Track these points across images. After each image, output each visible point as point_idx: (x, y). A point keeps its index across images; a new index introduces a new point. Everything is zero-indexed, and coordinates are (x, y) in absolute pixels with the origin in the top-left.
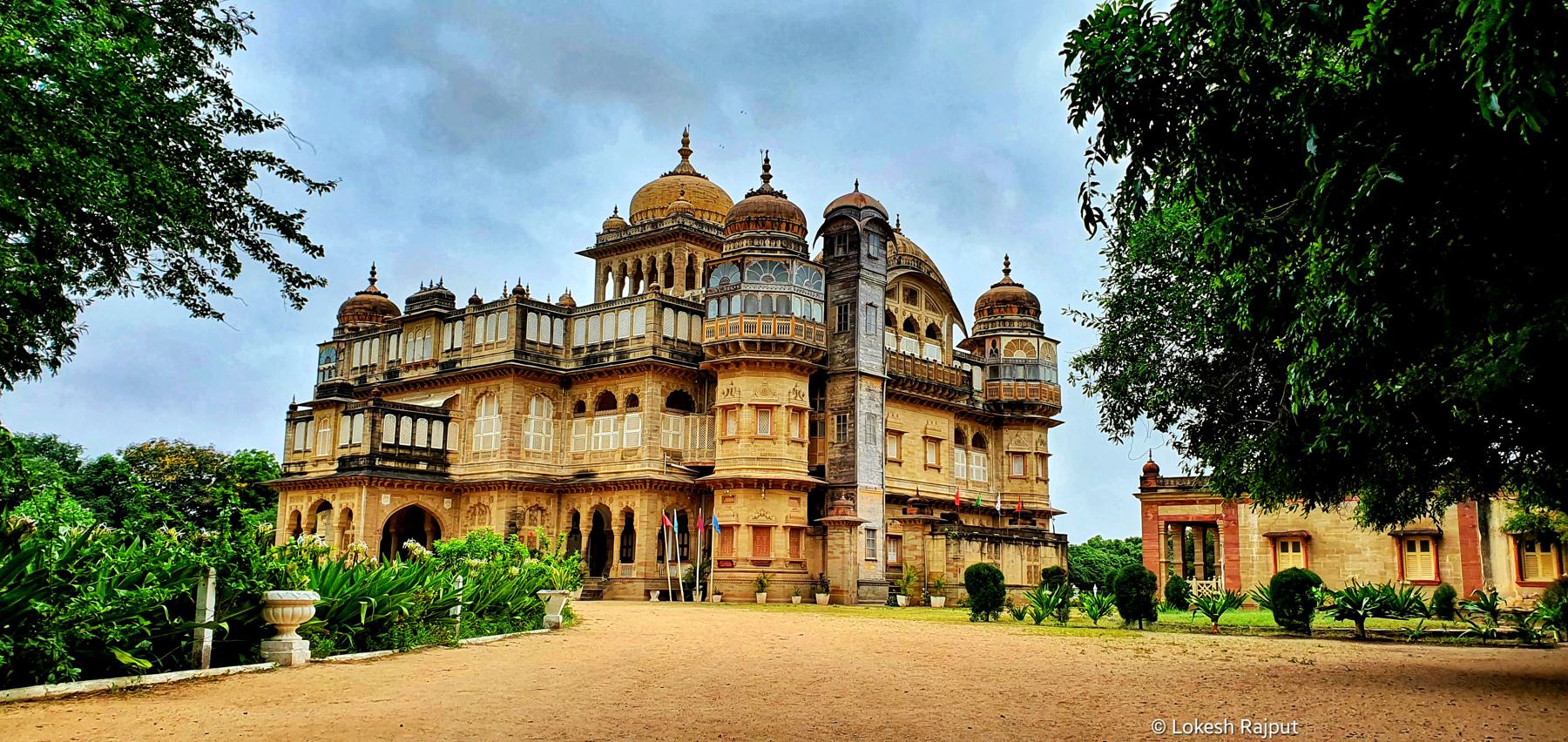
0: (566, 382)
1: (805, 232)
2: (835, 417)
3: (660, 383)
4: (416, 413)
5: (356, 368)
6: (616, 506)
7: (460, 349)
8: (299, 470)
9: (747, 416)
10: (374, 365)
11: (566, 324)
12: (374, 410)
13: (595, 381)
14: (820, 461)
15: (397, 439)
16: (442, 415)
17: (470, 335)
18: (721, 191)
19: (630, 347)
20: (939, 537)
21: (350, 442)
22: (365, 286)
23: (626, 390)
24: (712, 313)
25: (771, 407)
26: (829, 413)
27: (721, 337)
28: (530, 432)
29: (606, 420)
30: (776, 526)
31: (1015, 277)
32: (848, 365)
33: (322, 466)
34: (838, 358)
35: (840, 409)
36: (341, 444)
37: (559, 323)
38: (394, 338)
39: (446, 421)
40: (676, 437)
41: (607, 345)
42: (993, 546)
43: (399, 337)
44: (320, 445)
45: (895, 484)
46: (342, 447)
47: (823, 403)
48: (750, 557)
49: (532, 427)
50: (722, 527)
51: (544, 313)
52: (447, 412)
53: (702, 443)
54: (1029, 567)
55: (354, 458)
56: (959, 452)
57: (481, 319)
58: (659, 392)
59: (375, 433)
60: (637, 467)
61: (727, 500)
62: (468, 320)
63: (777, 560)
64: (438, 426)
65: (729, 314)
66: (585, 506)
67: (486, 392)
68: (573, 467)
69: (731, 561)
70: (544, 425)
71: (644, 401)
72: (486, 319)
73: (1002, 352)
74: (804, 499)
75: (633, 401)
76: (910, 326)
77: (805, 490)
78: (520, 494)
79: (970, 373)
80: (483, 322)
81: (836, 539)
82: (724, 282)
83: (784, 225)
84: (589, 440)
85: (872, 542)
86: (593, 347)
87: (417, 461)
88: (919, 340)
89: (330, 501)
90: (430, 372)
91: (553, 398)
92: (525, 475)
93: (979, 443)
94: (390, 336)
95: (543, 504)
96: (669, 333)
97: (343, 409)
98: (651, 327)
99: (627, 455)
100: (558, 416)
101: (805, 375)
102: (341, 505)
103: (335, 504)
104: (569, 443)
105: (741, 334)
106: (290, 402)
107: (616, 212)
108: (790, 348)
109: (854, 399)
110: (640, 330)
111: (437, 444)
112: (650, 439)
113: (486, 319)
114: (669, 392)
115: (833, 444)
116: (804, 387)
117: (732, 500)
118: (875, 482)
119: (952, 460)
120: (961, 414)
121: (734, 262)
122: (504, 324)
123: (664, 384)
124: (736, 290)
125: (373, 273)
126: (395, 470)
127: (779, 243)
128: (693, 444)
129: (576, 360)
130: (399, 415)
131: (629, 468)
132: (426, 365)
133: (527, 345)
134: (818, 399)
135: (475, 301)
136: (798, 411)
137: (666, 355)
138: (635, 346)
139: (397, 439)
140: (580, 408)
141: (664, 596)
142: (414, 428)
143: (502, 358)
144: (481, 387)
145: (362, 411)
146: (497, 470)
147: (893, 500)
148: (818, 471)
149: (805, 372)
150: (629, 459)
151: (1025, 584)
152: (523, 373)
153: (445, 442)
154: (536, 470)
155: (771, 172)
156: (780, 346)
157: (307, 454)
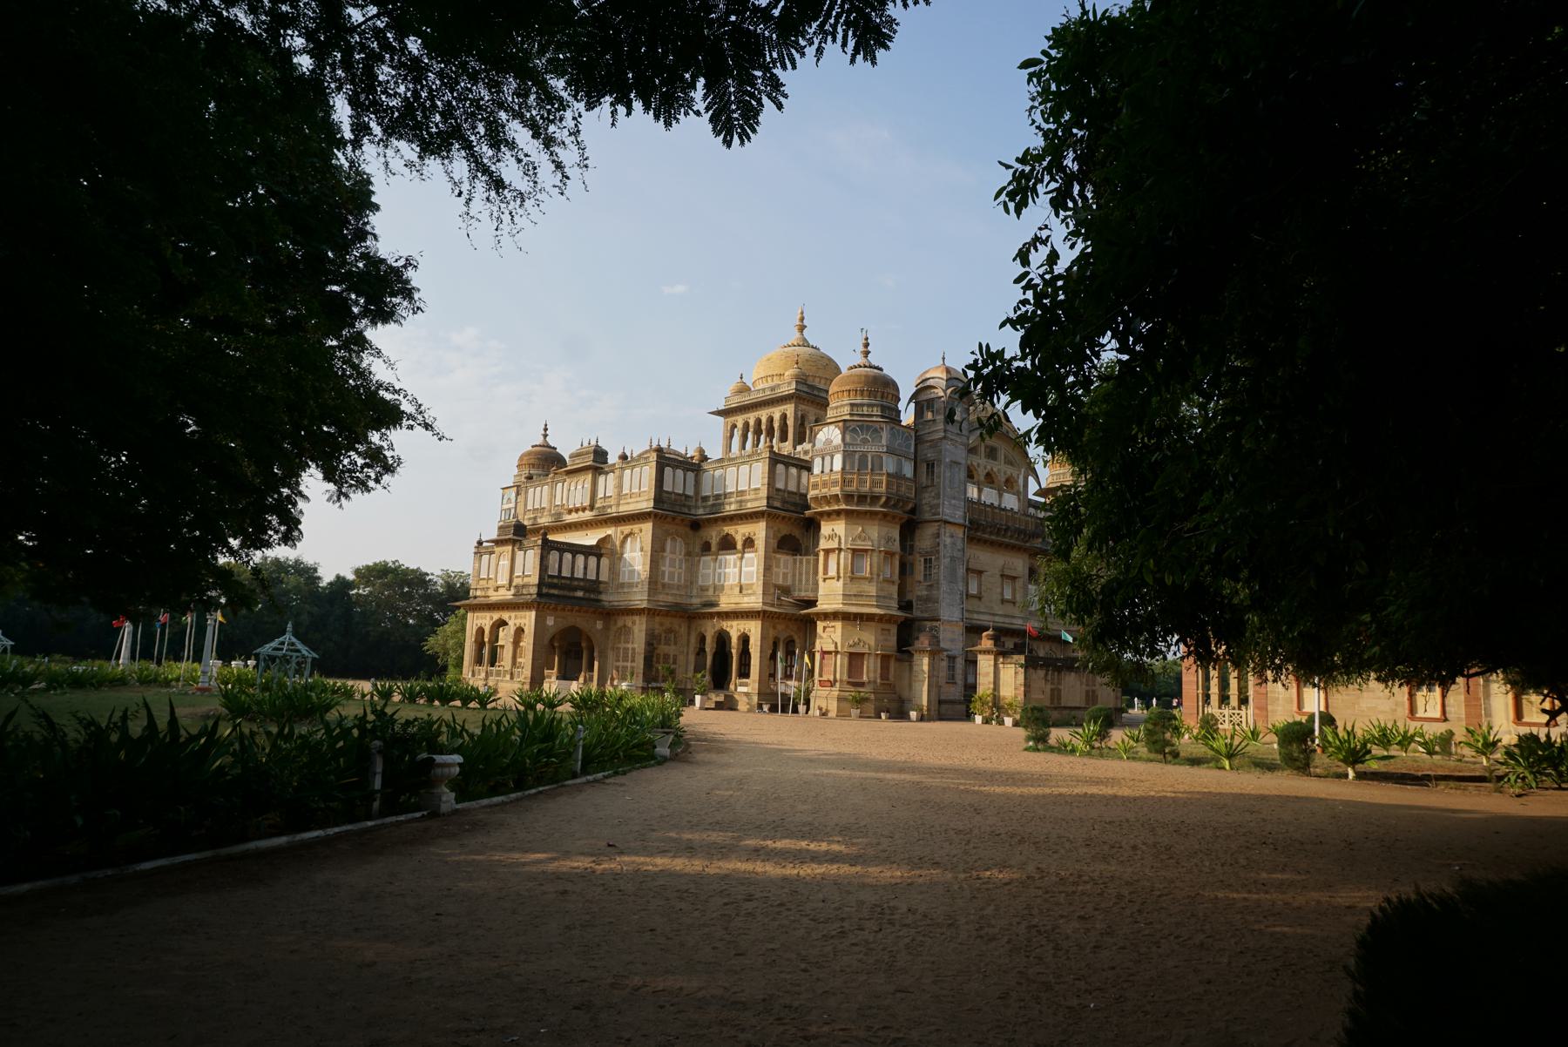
1: (899, 400)
6: (734, 629)
11: (696, 476)
14: (909, 597)
17: (620, 486)
18: (830, 360)
19: (748, 497)
22: (540, 441)
26: (918, 555)
28: (666, 568)
32: (934, 514)
33: (502, 591)
37: (691, 475)
38: (560, 485)
40: (785, 575)
44: (499, 575)
45: (976, 616)
47: (912, 547)
51: (677, 467)
52: (600, 549)
53: (807, 580)
54: (1087, 692)
60: (753, 599)
62: (617, 472)
64: (593, 561)
65: (831, 470)
74: (894, 630)
75: (749, 543)
76: (990, 479)
77: (895, 622)
78: (657, 619)
83: (879, 394)
85: (952, 668)
87: (575, 589)
90: (588, 515)
98: (766, 481)
100: (688, 554)
101: (896, 523)
103: (511, 623)
106: (478, 539)
108: (883, 499)
109: (939, 544)
111: (592, 576)
114: (780, 535)
116: (896, 534)
118: (957, 615)
120: (1033, 553)
123: (776, 529)
125: (546, 430)
128: (800, 580)
129: (704, 507)
131: (746, 599)
135: (624, 457)
138: (753, 497)
140: (706, 548)
144: (627, 529)
148: (906, 606)
149: (897, 520)
153: (598, 574)
154: (670, 599)
156: (875, 499)
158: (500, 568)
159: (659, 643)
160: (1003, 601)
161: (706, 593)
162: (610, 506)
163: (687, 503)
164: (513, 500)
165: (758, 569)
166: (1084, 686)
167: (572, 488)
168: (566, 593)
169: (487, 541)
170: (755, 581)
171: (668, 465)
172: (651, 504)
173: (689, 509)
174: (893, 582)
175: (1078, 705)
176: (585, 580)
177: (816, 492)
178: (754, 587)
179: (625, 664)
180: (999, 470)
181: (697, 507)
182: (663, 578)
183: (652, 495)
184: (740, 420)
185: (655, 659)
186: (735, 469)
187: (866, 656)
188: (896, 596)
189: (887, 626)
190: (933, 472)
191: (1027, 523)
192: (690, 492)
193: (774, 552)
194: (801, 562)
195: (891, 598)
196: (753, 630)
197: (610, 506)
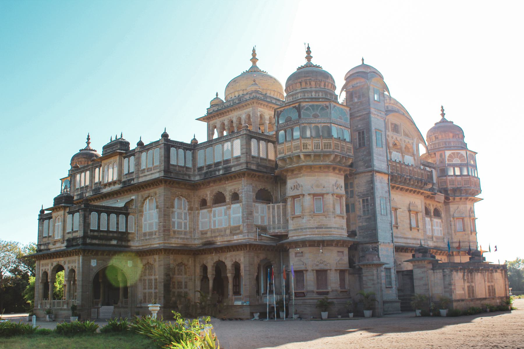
0: (195, 186)
1: (335, 88)
2: (361, 200)
3: (251, 184)
4: (109, 211)
5: (78, 189)
6: (228, 259)
7: (133, 172)
8: (46, 248)
9: (307, 201)
10: (87, 187)
11: (193, 153)
12: (84, 210)
13: (212, 186)
14: (353, 228)
15: (99, 227)
16: (124, 211)
17: (138, 164)
19: (232, 164)
20: (438, 271)
23: (231, 191)
24: (281, 139)
26: (357, 198)
27: (287, 154)
28: (175, 220)
29: (220, 210)
30: (330, 270)
31: (448, 118)
32: (367, 167)
33: (58, 245)
34: (361, 163)
35: (364, 195)
37: (189, 153)
38: (97, 170)
39: (127, 215)
40: (263, 218)
41: (218, 164)
42: (469, 274)
43: (100, 169)
46: (69, 233)
47: (352, 192)
48: (315, 290)
49: (176, 217)
50: (296, 272)
51: (179, 148)
52: (127, 210)
53: (279, 221)
54: (489, 286)
55: (74, 239)
56: (428, 219)
57: (144, 154)
58: (251, 190)
59: (86, 223)
60: (240, 236)
61: (298, 255)
62: (137, 155)
63: (332, 291)
64: (122, 218)
66: (210, 261)
67: (149, 196)
68: (201, 239)
69: (303, 293)
70: (183, 214)
71: (242, 196)
72: (147, 153)
73: (446, 160)
74: (346, 251)
75: (235, 197)
77: (347, 246)
78: (172, 257)
80: (145, 156)
81: (368, 275)
82: (288, 120)
84: (210, 222)
85: (388, 276)
86: (209, 166)
87: (111, 239)
88: (402, 153)
89: (63, 265)
90: (117, 187)
91: (187, 197)
92: (173, 245)
93: (437, 214)
94: (95, 169)
95: (185, 261)
96: (254, 153)
97: (68, 210)
98: (244, 150)
99: (235, 230)
100: (191, 209)
101: (342, 175)
102: (69, 268)
104: (198, 225)
105: (301, 150)
110: (237, 152)
111: (122, 229)
112: (248, 219)
113: (147, 153)
114: (257, 190)
115: (361, 216)
117: (301, 254)
119: (424, 224)
121: (294, 107)
122: (158, 154)
124: (297, 123)
126: (98, 245)
127: (320, 94)
128: (274, 222)
129: (200, 175)
130: (99, 213)
131: (235, 237)
132: (114, 183)
133: (171, 167)
134: (349, 190)
135: (140, 144)
136: (340, 196)
137: (254, 167)
138: (235, 163)
139: (99, 227)
140: (204, 204)
141: (263, 316)
142: (108, 220)
143: (157, 176)
144: (146, 193)
146: (156, 243)
147: (399, 249)
149: (342, 173)
150: (234, 232)
151: (488, 297)
152: (169, 183)
153: (127, 227)
154: (180, 241)
155: (311, 55)
156: (326, 155)
157: (50, 238)
158: (56, 228)
159: (174, 274)
161: (205, 236)
162: (133, 179)
163: (188, 173)
164: (68, 186)
165: (243, 215)
166: (486, 283)
167: (106, 169)
168: (104, 242)
169: (47, 210)
170: (241, 223)
171: (173, 146)
172: (162, 174)
173: (189, 177)
174: (343, 217)
175: (484, 297)
176: (117, 232)
177: (283, 155)
178: (241, 228)
179: (150, 291)
180: (400, 139)
181: (195, 176)
182: (174, 227)
183: (162, 167)
184: (218, 121)
185: (171, 286)
186: (220, 145)
187: (329, 271)
188: (345, 227)
189: (341, 249)
190: (363, 138)
191: (422, 174)
192: (189, 165)
193: (254, 202)
194: (273, 208)
195: (343, 229)
196: (242, 259)
197: (133, 179)
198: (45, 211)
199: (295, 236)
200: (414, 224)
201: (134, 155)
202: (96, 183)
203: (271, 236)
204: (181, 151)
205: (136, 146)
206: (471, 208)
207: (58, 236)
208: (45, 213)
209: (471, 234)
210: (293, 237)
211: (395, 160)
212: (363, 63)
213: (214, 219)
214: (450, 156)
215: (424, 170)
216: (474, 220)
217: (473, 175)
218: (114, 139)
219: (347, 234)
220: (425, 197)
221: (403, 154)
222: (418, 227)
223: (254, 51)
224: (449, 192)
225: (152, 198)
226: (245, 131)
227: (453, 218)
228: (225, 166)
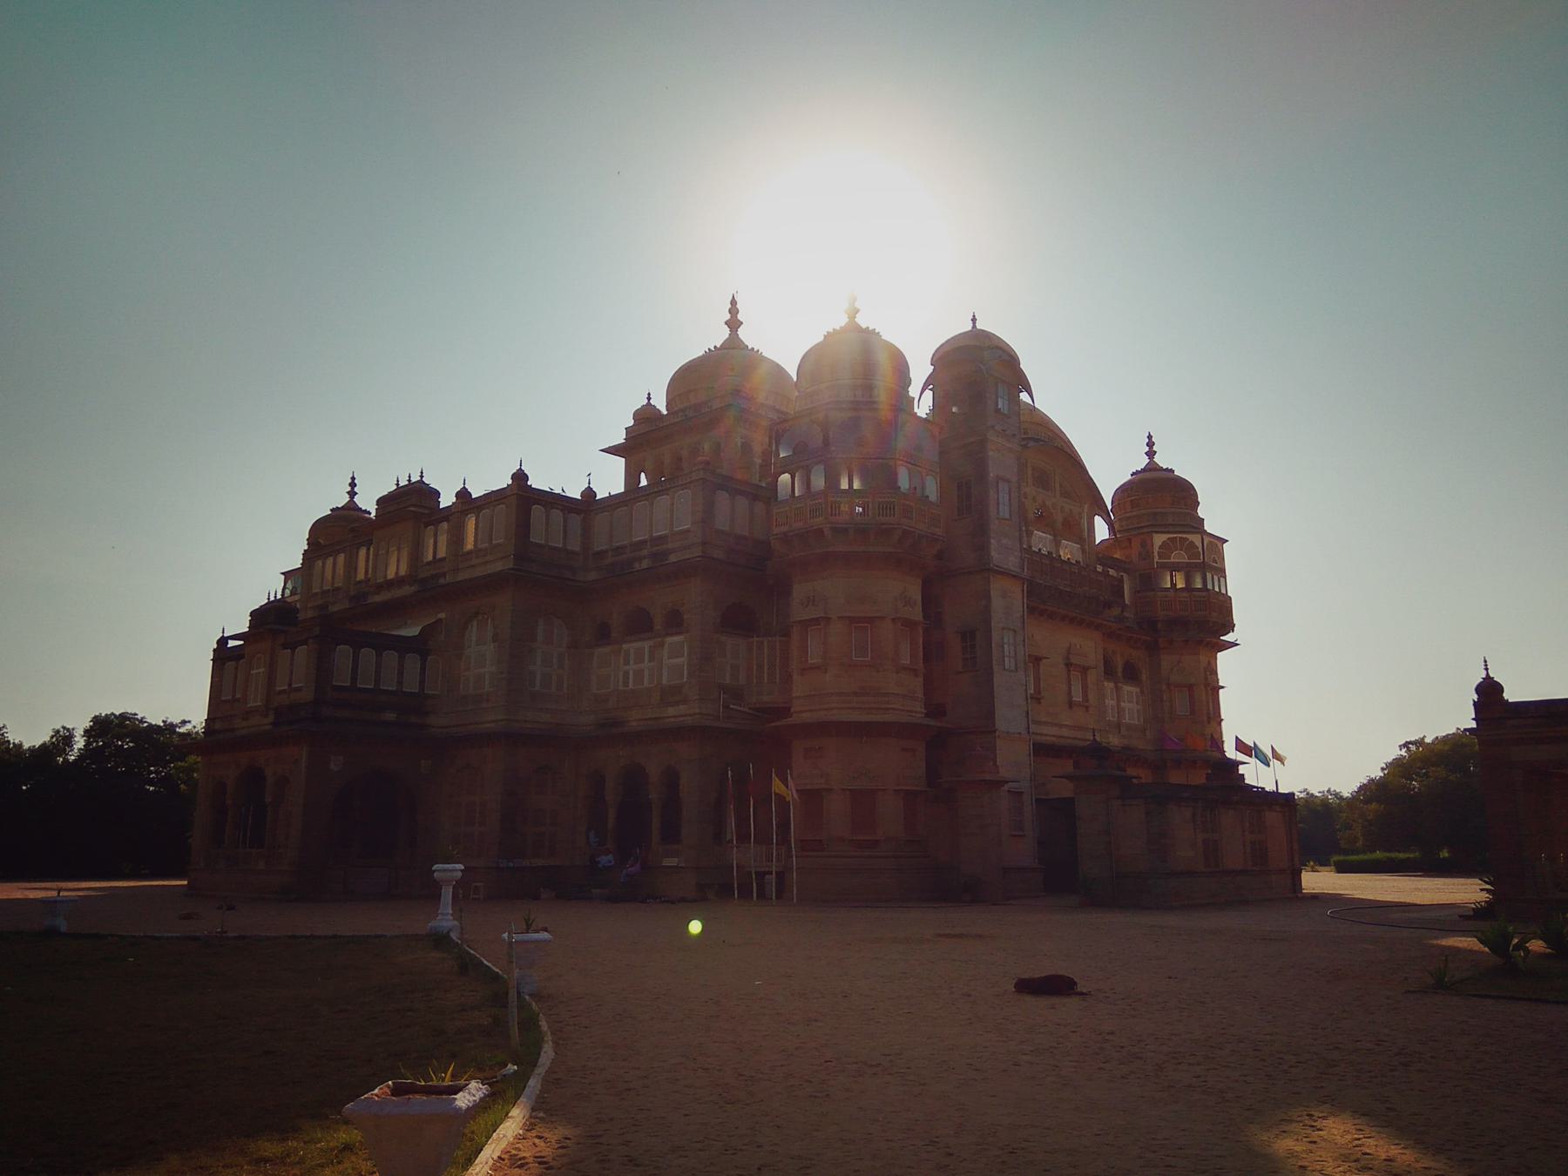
7: (444, 559)
17: (457, 538)
21: (290, 685)
25: (871, 620)
31: (1162, 460)
36: (278, 689)
37: (575, 521)
38: (363, 552)
43: (368, 549)
46: (280, 692)
56: (1109, 685)
60: (682, 709)
64: (412, 663)
69: (821, 841)
73: (1156, 554)
75: (675, 622)
79: (1121, 580)
86: (620, 550)
88: (1055, 536)
90: (407, 590)
93: (1131, 674)
94: (358, 549)
107: (649, 399)
111: (411, 686)
116: (915, 592)
131: (671, 711)
132: (399, 581)
135: (463, 494)
136: (909, 624)
140: (603, 634)
143: (498, 567)
145: (305, 642)
147: (1043, 750)
148: (935, 710)
153: (422, 682)
160: (1071, 704)
162: (444, 575)
177: (784, 529)
188: (920, 694)
192: (575, 545)
197: (444, 575)
198: (230, 641)
199: (806, 711)
200: (1078, 697)
201: (446, 519)
202: (360, 582)
203: (750, 708)
204: (557, 515)
205: (454, 500)
206: (1209, 663)
207: (256, 701)
208: (229, 646)
209: (1209, 722)
210: (803, 713)
211: (1040, 550)
212: (974, 326)
213: (627, 667)
214: (1164, 545)
215: (1106, 574)
216: (1216, 688)
217: (1217, 589)
218: (403, 483)
219: (925, 709)
220: (1104, 634)
221: (1059, 538)
222: (1087, 701)
223: (733, 302)
224: (1159, 626)
225: (486, 616)
226: (702, 472)
227: (1169, 685)
228: (655, 549)
